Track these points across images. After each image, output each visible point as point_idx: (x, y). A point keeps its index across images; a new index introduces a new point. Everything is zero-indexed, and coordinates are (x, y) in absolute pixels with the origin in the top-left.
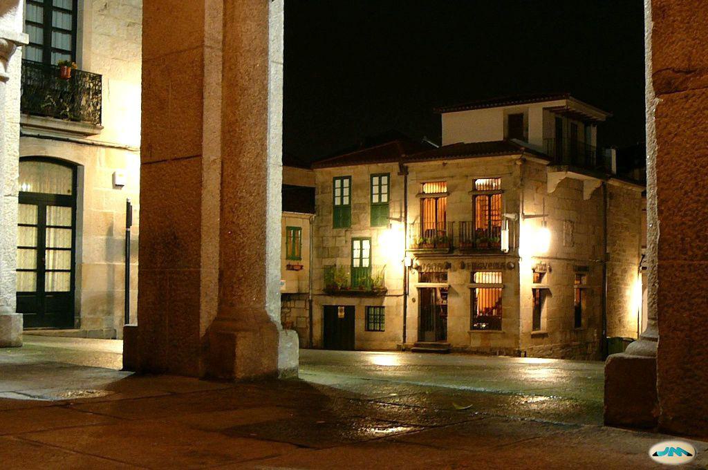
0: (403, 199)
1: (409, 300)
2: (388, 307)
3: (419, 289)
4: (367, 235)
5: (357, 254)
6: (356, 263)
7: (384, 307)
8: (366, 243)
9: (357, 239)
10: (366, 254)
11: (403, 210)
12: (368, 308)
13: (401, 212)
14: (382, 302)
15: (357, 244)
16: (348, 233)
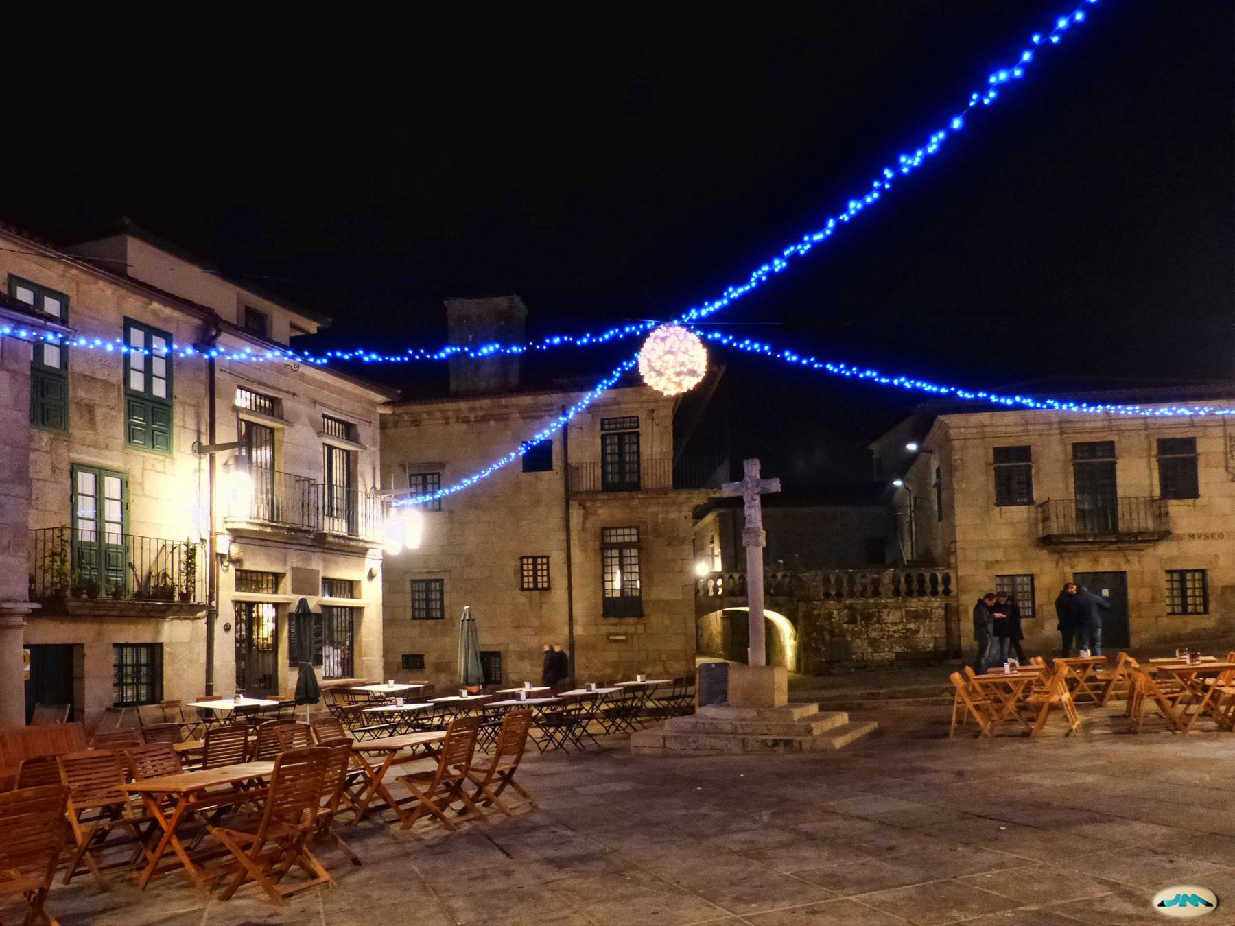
0: (206, 401)
1: (218, 626)
2: (171, 644)
3: (237, 603)
4: (115, 462)
5: (86, 508)
6: (86, 531)
7: (161, 645)
8: (112, 486)
9: (87, 468)
10: (112, 511)
11: (204, 428)
12: (120, 647)
13: (199, 432)
14: (157, 633)
15: (86, 482)
16: (62, 450)
